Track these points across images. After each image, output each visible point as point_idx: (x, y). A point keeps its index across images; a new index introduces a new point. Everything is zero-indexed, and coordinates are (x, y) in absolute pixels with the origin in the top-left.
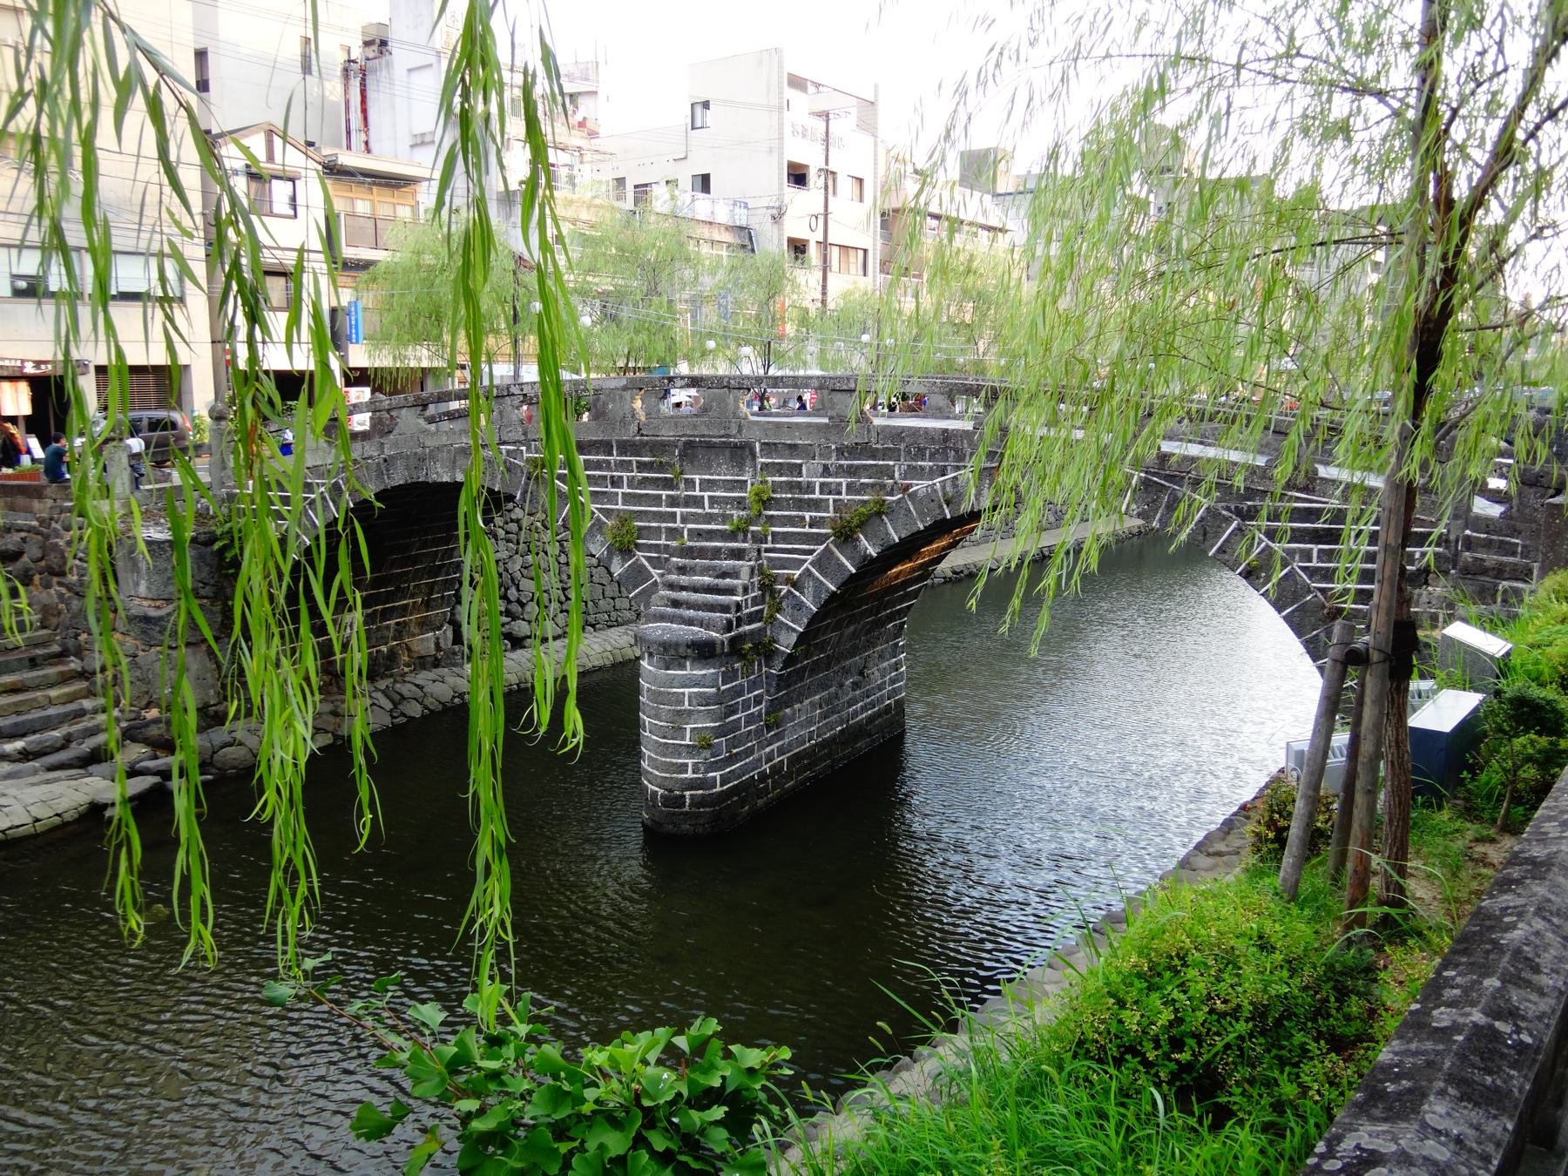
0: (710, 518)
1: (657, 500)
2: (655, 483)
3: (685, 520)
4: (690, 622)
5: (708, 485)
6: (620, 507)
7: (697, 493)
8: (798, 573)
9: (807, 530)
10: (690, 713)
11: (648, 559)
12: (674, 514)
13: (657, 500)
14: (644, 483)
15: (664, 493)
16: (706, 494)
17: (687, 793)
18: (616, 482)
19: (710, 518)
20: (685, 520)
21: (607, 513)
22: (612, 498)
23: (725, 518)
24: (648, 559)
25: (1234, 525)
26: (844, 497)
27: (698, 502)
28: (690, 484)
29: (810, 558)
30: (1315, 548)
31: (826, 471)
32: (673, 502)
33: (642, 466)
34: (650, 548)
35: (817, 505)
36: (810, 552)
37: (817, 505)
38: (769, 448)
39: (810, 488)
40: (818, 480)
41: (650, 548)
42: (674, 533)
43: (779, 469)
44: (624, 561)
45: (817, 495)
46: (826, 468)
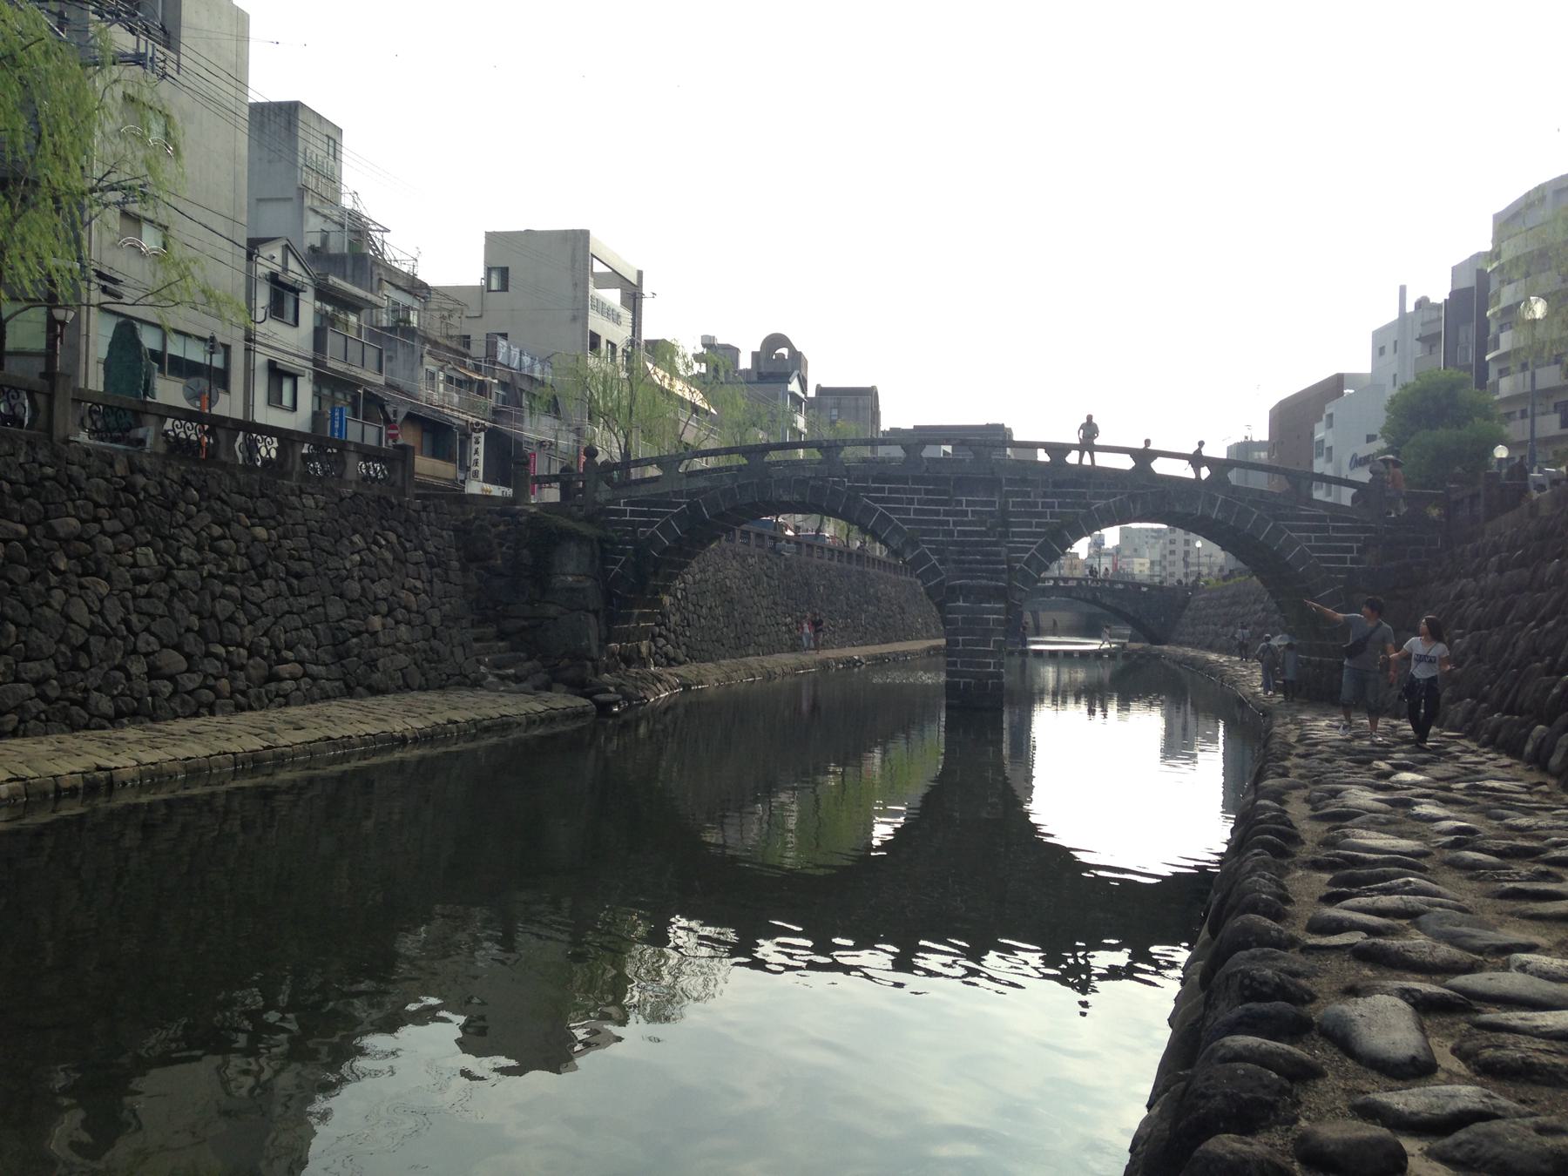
0: (970, 523)
1: (937, 513)
3: (955, 523)
5: (969, 503)
6: (912, 516)
7: (964, 508)
8: (1027, 556)
9: (1034, 529)
10: (992, 630)
11: (929, 549)
12: (948, 521)
13: (937, 513)
14: (928, 502)
16: (969, 509)
17: (990, 682)
18: (911, 502)
19: (970, 523)
20: (955, 523)
21: (904, 521)
22: (907, 511)
23: (983, 523)
24: (929, 549)
25: (1271, 524)
26: (1057, 510)
27: (965, 513)
28: (959, 503)
29: (1035, 546)
30: (1313, 535)
31: (1045, 495)
32: (947, 513)
33: (927, 492)
34: (930, 542)
35: (1041, 515)
36: (1035, 543)
38: (1011, 482)
39: (1035, 505)
40: (1040, 500)
41: (930, 542)
42: (951, 533)
43: (1017, 494)
44: (913, 551)
45: (1040, 509)
46: (1045, 493)
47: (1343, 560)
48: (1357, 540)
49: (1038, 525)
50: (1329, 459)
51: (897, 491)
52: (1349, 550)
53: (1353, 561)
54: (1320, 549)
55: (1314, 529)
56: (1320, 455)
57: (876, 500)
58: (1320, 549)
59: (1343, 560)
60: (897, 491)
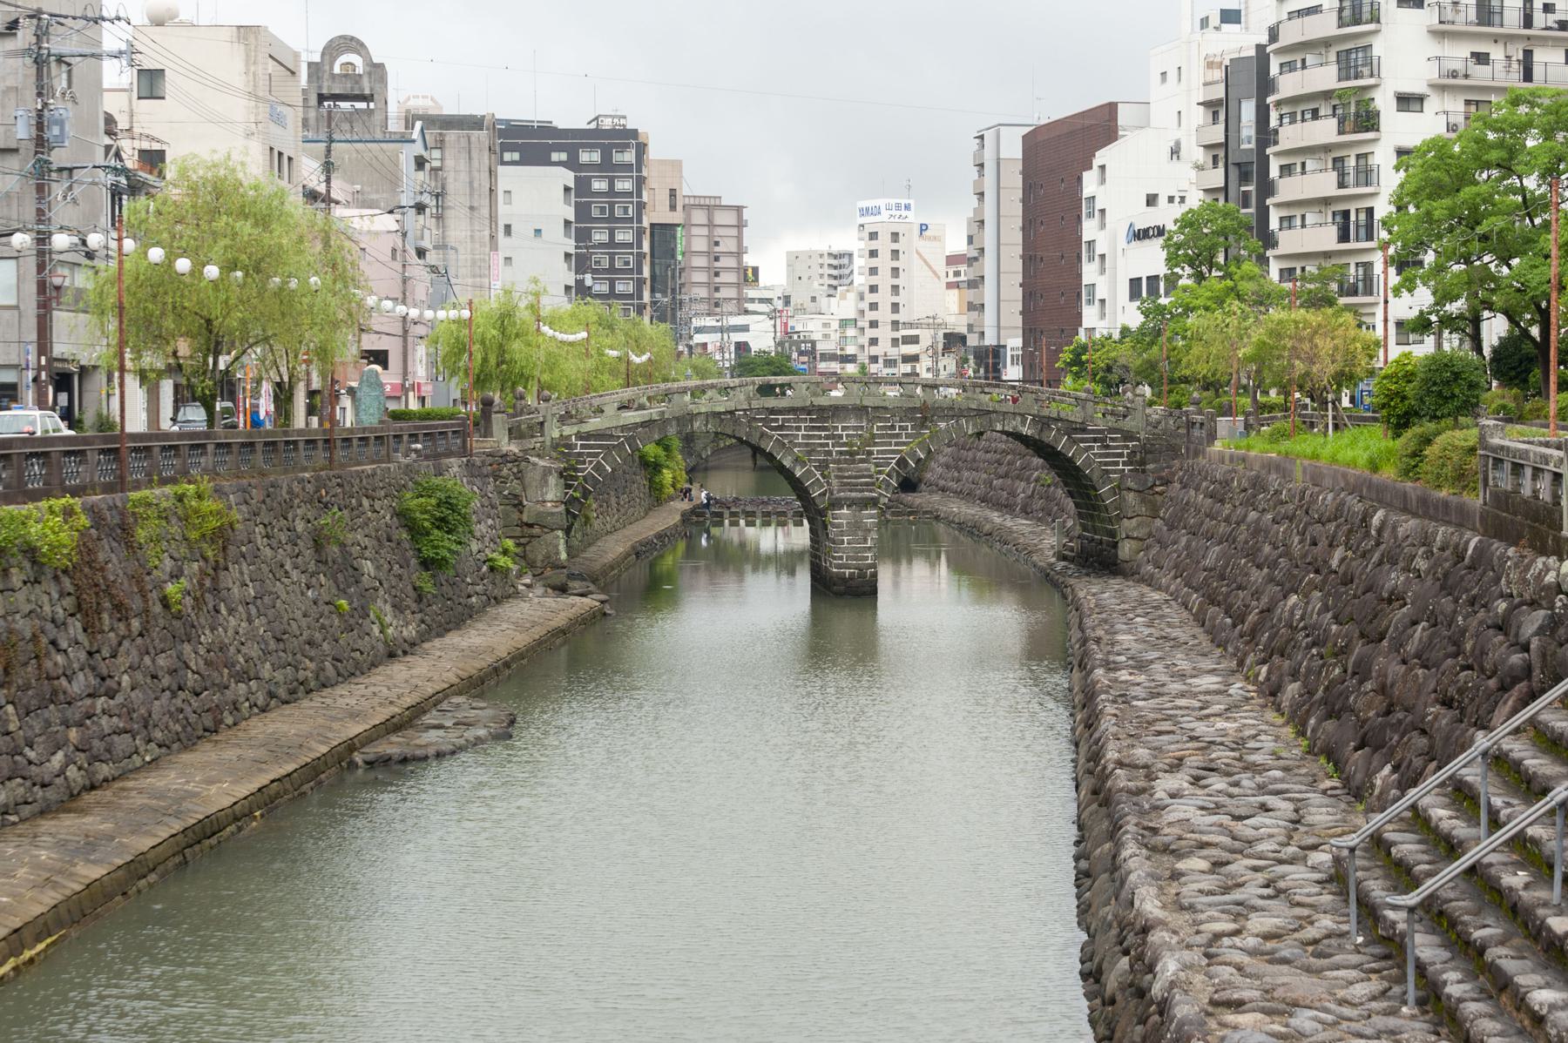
1: (820, 437)
2: (819, 428)
4: (863, 491)
5: (844, 428)
13: (820, 437)
14: (813, 428)
15: (823, 433)
18: (799, 429)
27: (841, 437)
31: (901, 421)
32: (827, 437)
33: (812, 420)
35: (898, 436)
37: (898, 436)
42: (829, 453)
43: (880, 419)
47: (1117, 464)
48: (1127, 447)
49: (897, 444)
50: (1103, 226)
51: (789, 420)
52: (1121, 455)
53: (1124, 464)
54: (1101, 456)
55: (1095, 440)
56: (1090, 215)
57: (773, 429)
58: (1101, 456)
59: (1117, 464)
60: (789, 420)
